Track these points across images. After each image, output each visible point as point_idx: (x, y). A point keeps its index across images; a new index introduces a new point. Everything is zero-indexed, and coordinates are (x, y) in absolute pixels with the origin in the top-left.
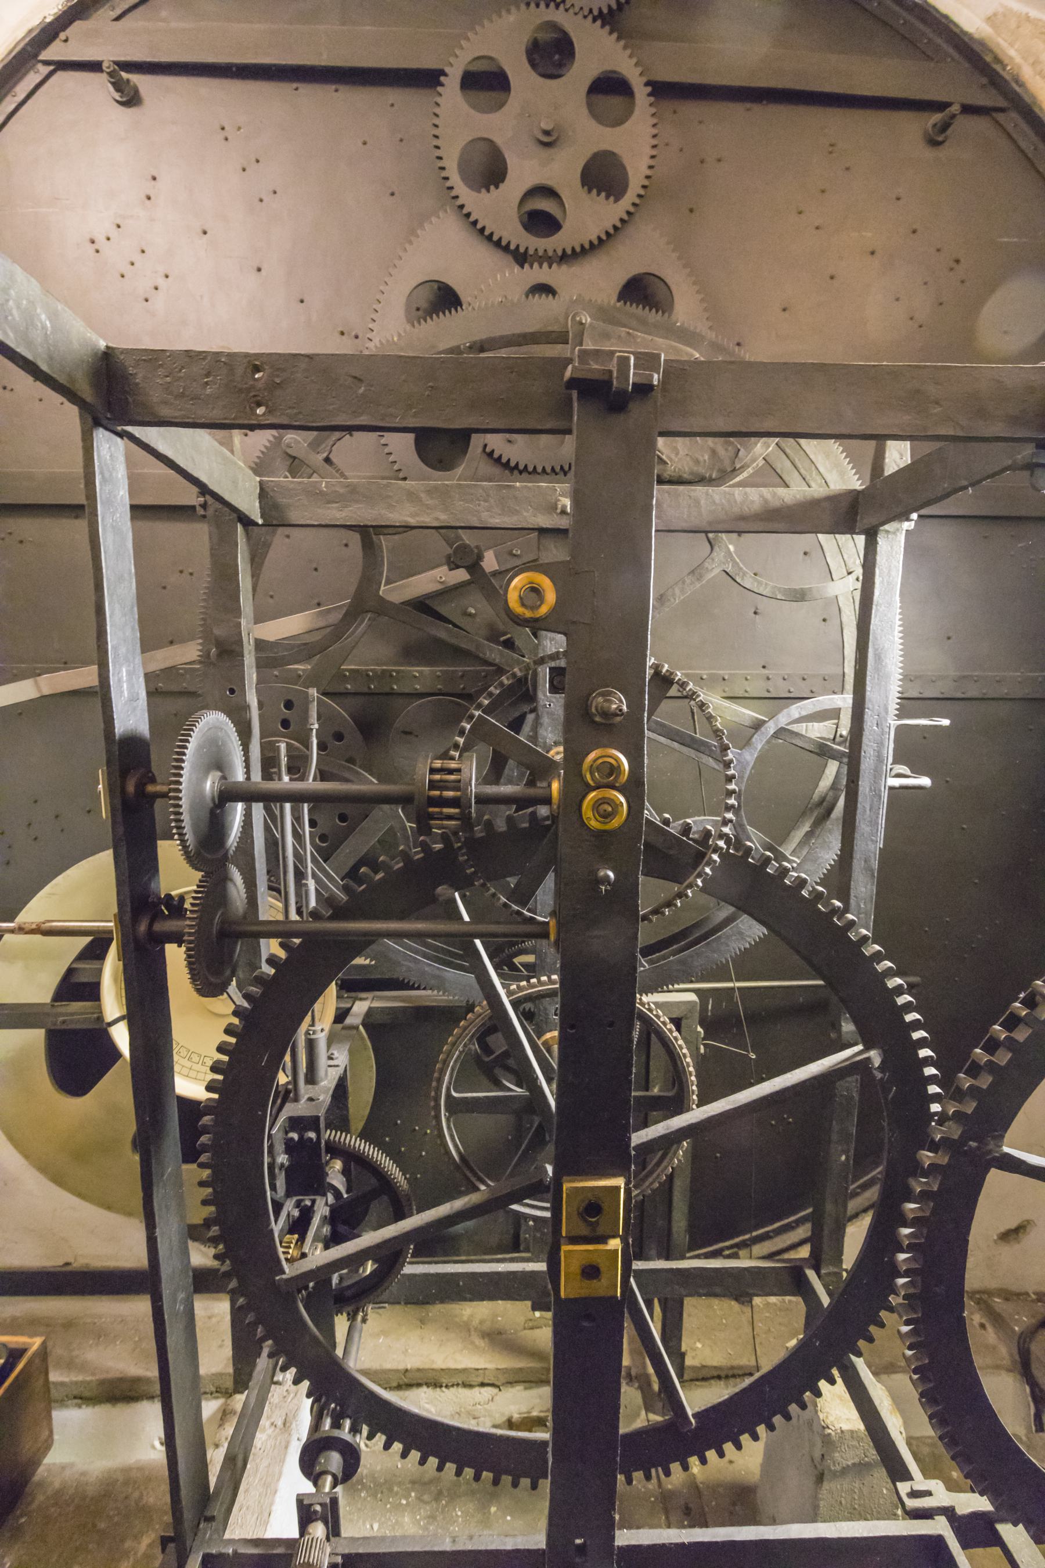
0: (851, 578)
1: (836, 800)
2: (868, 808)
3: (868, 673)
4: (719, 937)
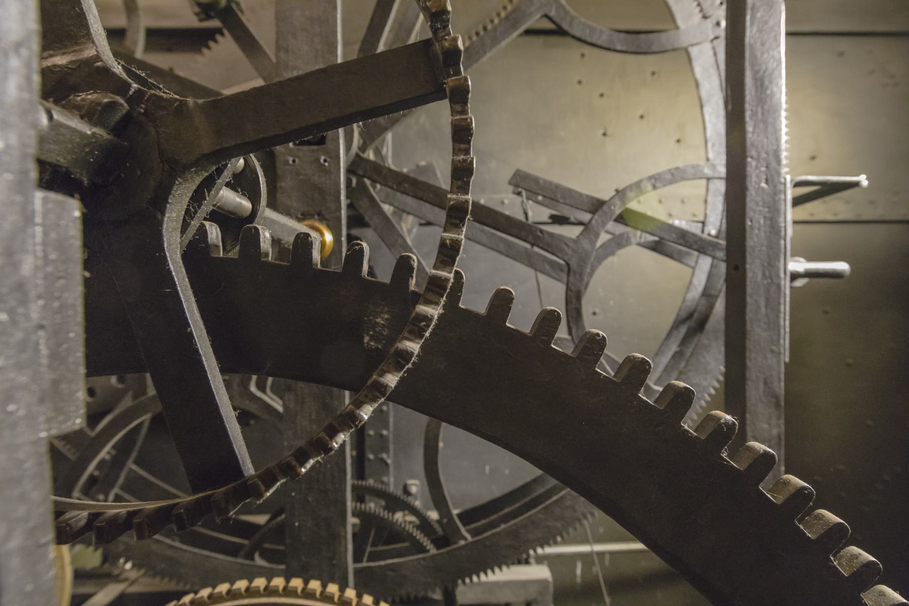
0: (710, 23)
1: (711, 307)
2: (763, 304)
3: (747, 106)
4: (562, 498)
